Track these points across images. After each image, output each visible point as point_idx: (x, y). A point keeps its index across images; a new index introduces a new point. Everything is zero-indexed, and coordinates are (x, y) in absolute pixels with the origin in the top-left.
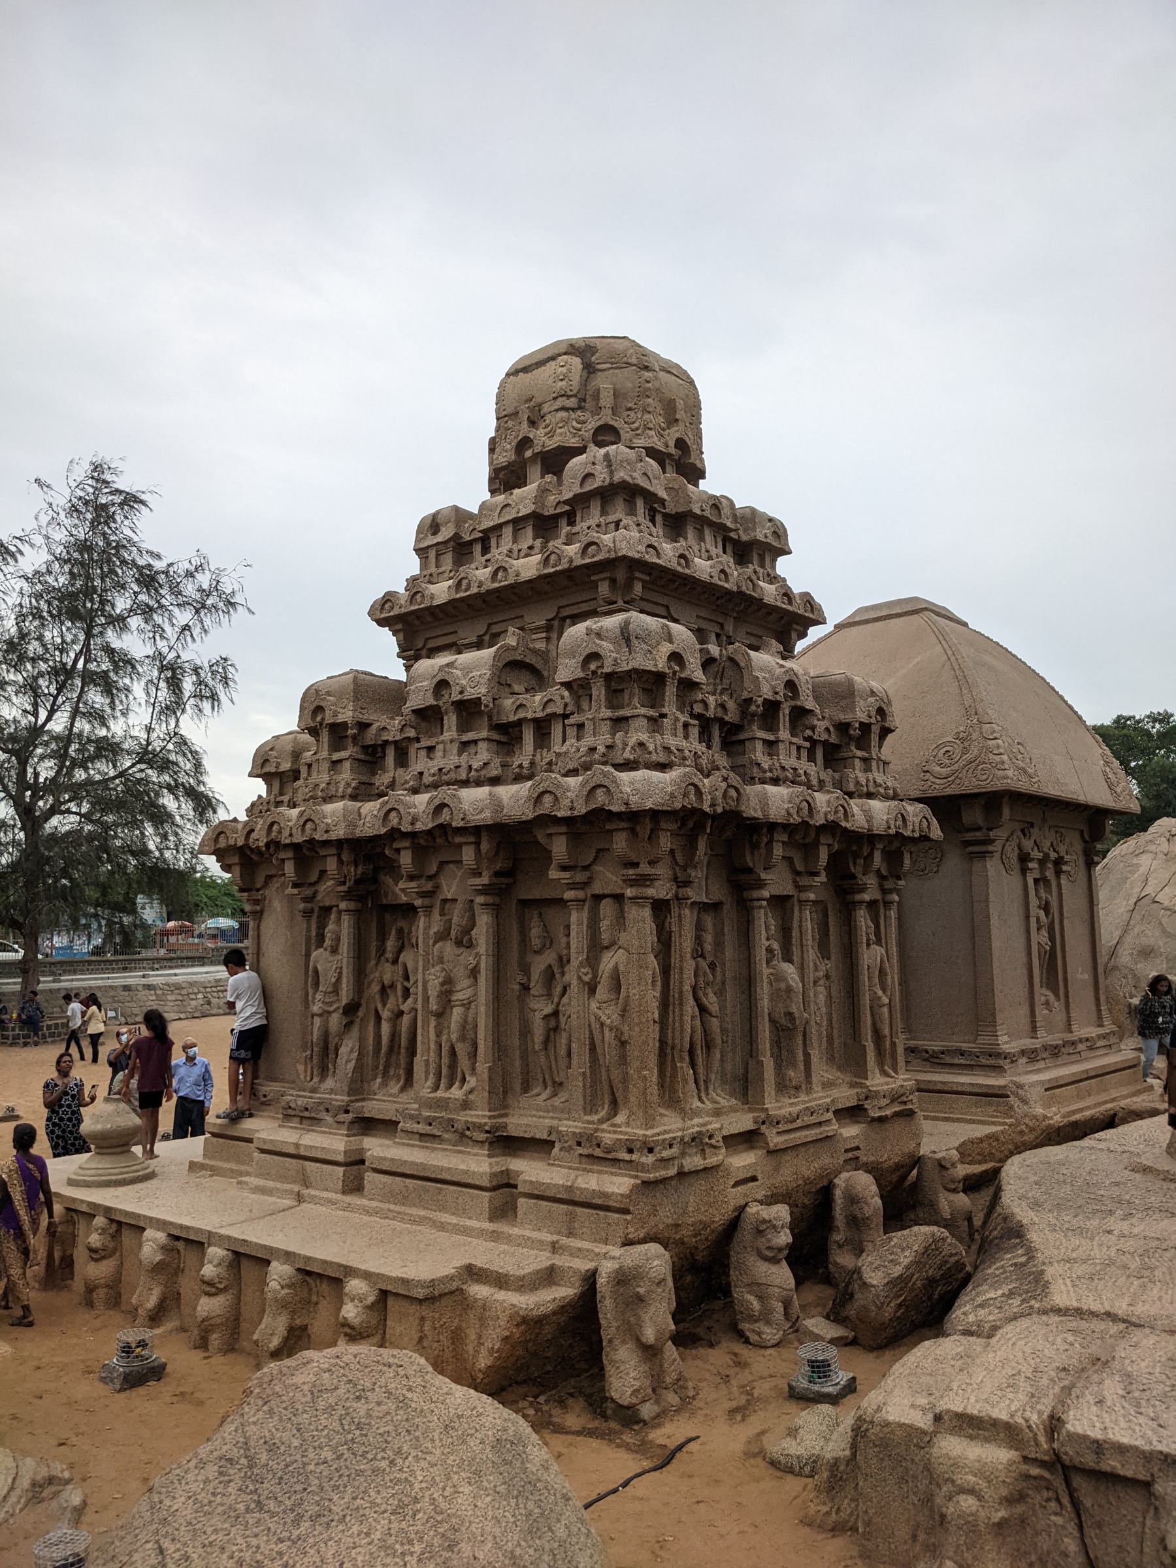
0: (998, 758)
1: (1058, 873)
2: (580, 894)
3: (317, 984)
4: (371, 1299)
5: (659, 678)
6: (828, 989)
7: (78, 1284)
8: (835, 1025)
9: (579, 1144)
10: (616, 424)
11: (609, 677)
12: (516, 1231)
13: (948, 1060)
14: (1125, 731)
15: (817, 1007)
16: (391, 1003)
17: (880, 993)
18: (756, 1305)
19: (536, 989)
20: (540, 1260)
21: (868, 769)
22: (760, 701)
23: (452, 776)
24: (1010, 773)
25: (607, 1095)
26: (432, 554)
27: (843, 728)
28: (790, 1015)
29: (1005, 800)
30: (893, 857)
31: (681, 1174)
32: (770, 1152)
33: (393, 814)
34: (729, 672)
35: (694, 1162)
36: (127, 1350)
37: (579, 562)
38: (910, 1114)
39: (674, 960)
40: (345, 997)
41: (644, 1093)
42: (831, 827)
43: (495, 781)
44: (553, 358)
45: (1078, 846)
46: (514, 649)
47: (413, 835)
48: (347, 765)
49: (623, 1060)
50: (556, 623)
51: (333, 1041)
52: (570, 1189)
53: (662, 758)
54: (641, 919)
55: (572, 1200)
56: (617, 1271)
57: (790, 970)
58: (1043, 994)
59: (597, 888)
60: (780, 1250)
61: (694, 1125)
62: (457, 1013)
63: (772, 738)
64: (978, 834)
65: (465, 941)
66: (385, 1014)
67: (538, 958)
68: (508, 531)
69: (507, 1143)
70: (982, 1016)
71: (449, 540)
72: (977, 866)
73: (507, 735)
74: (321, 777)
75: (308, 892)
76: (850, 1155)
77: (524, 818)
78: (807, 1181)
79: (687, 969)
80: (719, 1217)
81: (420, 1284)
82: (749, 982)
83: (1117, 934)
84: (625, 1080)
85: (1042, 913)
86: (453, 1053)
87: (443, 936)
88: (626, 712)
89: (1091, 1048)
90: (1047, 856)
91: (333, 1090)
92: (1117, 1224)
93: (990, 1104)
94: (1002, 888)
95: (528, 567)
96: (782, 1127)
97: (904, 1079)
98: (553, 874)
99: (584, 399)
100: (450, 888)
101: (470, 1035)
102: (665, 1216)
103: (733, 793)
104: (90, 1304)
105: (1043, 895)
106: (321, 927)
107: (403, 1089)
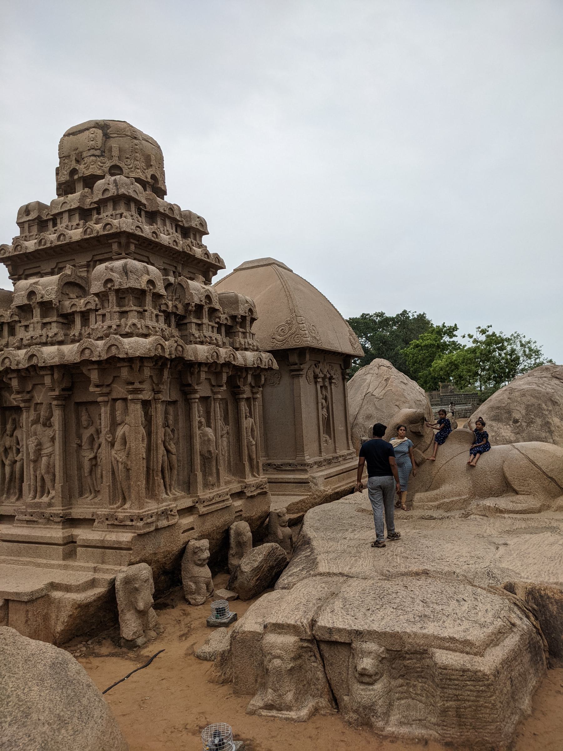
0: (303, 332)
1: (331, 383)
2: (106, 399)
6: (228, 438)
8: (231, 455)
9: (107, 519)
10: (121, 165)
11: (117, 291)
12: (76, 564)
13: (284, 468)
14: (366, 321)
17: (251, 439)
18: (193, 586)
19: (85, 446)
20: (89, 576)
21: (245, 337)
22: (193, 304)
23: (38, 340)
24: (309, 339)
25: (120, 495)
26: (26, 226)
27: (234, 318)
28: (209, 452)
29: (307, 351)
30: (257, 377)
31: (157, 530)
32: (200, 516)
33: (7, 360)
34: (179, 290)
35: (164, 523)
37: (102, 233)
38: (265, 493)
39: (153, 428)
41: (138, 493)
42: (227, 364)
43: (61, 343)
44: (87, 129)
45: (339, 372)
46: (70, 276)
47: (18, 371)
49: (128, 478)
50: (92, 263)
52: (103, 541)
53: (145, 331)
54: (136, 410)
55: (103, 546)
56: (125, 578)
58: (324, 437)
59: (114, 395)
60: (204, 560)
61: (163, 506)
62: (44, 460)
63: (200, 322)
64: (296, 366)
65: (47, 424)
67: (86, 431)
68: (66, 216)
69: (71, 522)
70: (298, 447)
71: (34, 218)
72: (296, 380)
73: (67, 319)
76: (238, 514)
77: (75, 362)
78: (218, 528)
79: (160, 433)
80: (176, 548)
81: (25, 594)
82: (190, 437)
83: (357, 409)
84: (129, 488)
85: (324, 401)
86: (43, 479)
89: (345, 460)
90: (325, 376)
92: (349, 535)
93: (302, 486)
94: (306, 390)
95: (76, 234)
96: (205, 504)
97: (262, 478)
98: (92, 389)
100: (39, 397)
102: (149, 550)
103: (180, 348)
105: (324, 393)
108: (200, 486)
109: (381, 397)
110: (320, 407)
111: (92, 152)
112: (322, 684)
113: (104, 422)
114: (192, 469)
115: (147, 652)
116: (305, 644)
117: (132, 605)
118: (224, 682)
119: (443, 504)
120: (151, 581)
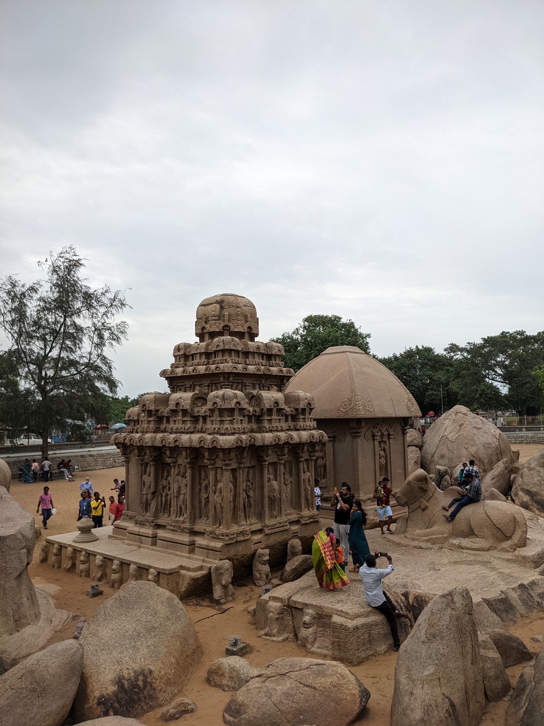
1: (389, 438)
2: (212, 467)
3: (144, 485)
4: (156, 574)
5: (233, 409)
6: (292, 486)
7: (77, 571)
12: (195, 556)
14: (504, 339)
15: (287, 491)
16: (165, 491)
17: (308, 486)
18: (258, 576)
20: (199, 564)
21: (305, 421)
22: (265, 409)
23: (180, 430)
25: (218, 521)
26: (178, 357)
27: (297, 410)
28: (274, 496)
31: (237, 542)
32: (266, 535)
34: (258, 400)
35: (241, 538)
36: (93, 587)
37: (214, 372)
38: (317, 522)
39: (238, 484)
41: (227, 521)
42: (287, 443)
43: (192, 433)
44: (211, 304)
46: (198, 394)
47: (169, 447)
48: (152, 422)
51: (149, 502)
54: (227, 475)
56: (216, 567)
57: (275, 483)
59: (217, 465)
60: (265, 561)
61: (241, 529)
62: (182, 496)
63: (270, 418)
65: (184, 476)
66: (164, 495)
67: (204, 482)
68: (198, 355)
69: (194, 533)
71: (183, 354)
72: (355, 440)
73: (195, 419)
74: (145, 425)
75: (142, 458)
76: (295, 534)
78: (279, 542)
79: (243, 485)
80: (249, 552)
81: (167, 570)
82: (262, 487)
83: (435, 449)
84: (222, 517)
86: (181, 507)
87: (178, 474)
91: (149, 516)
95: (202, 369)
96: (269, 528)
98: (205, 461)
99: (220, 317)
100: (180, 462)
101: (185, 503)
102: (232, 552)
103: (253, 440)
104: (81, 576)
106: (146, 468)
107: (169, 516)
108: (267, 517)
109: (454, 440)
110: (377, 457)
111: (214, 318)
112: (291, 627)
113: (211, 478)
114: (263, 507)
115: (225, 607)
116: (285, 608)
117: (220, 582)
118: (254, 624)
119: (431, 539)
120: (231, 570)
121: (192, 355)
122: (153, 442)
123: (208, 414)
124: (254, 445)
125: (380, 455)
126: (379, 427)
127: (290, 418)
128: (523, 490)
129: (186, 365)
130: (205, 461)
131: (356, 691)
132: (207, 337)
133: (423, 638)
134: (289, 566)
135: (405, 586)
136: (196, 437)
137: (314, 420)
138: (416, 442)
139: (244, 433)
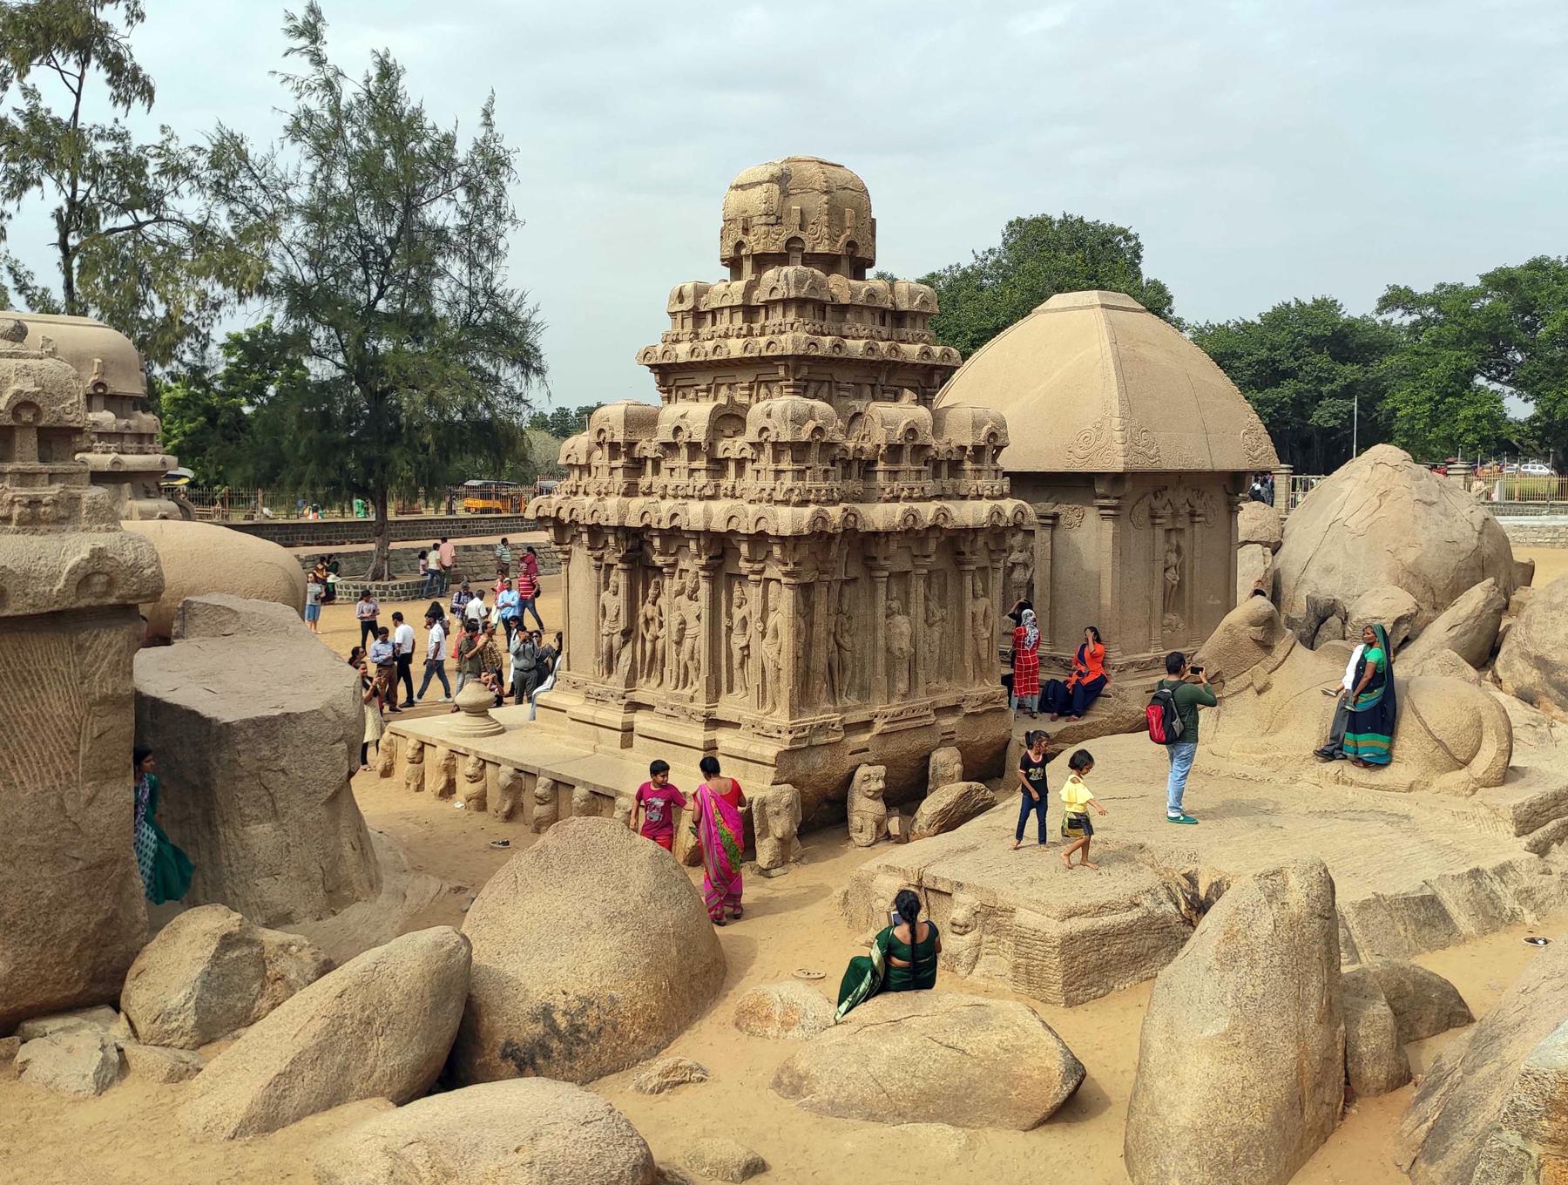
2: (757, 577)
3: (604, 615)
19: (737, 630)
26: (679, 317)
31: (811, 747)
37: (764, 353)
40: (622, 624)
44: (760, 183)
51: (615, 653)
59: (767, 574)
65: (692, 597)
66: (648, 637)
68: (727, 312)
69: (713, 723)
74: (603, 478)
75: (598, 554)
86: (686, 667)
87: (680, 593)
88: (782, 466)
95: (735, 348)
98: (742, 564)
103: (851, 518)
106: (607, 577)
110: (1160, 566)
121: (713, 312)
122: (623, 516)
123: (748, 453)
124: (856, 531)
125: (1166, 562)
126: (1168, 495)
127: (945, 469)
128: (1525, 656)
129: (697, 335)
130: (742, 564)
131: (1056, 1065)
132: (748, 266)
133: (1210, 960)
134: (930, 807)
135: (1193, 857)
136: (720, 508)
137: (1006, 474)
138: (1262, 535)
139: (834, 502)
